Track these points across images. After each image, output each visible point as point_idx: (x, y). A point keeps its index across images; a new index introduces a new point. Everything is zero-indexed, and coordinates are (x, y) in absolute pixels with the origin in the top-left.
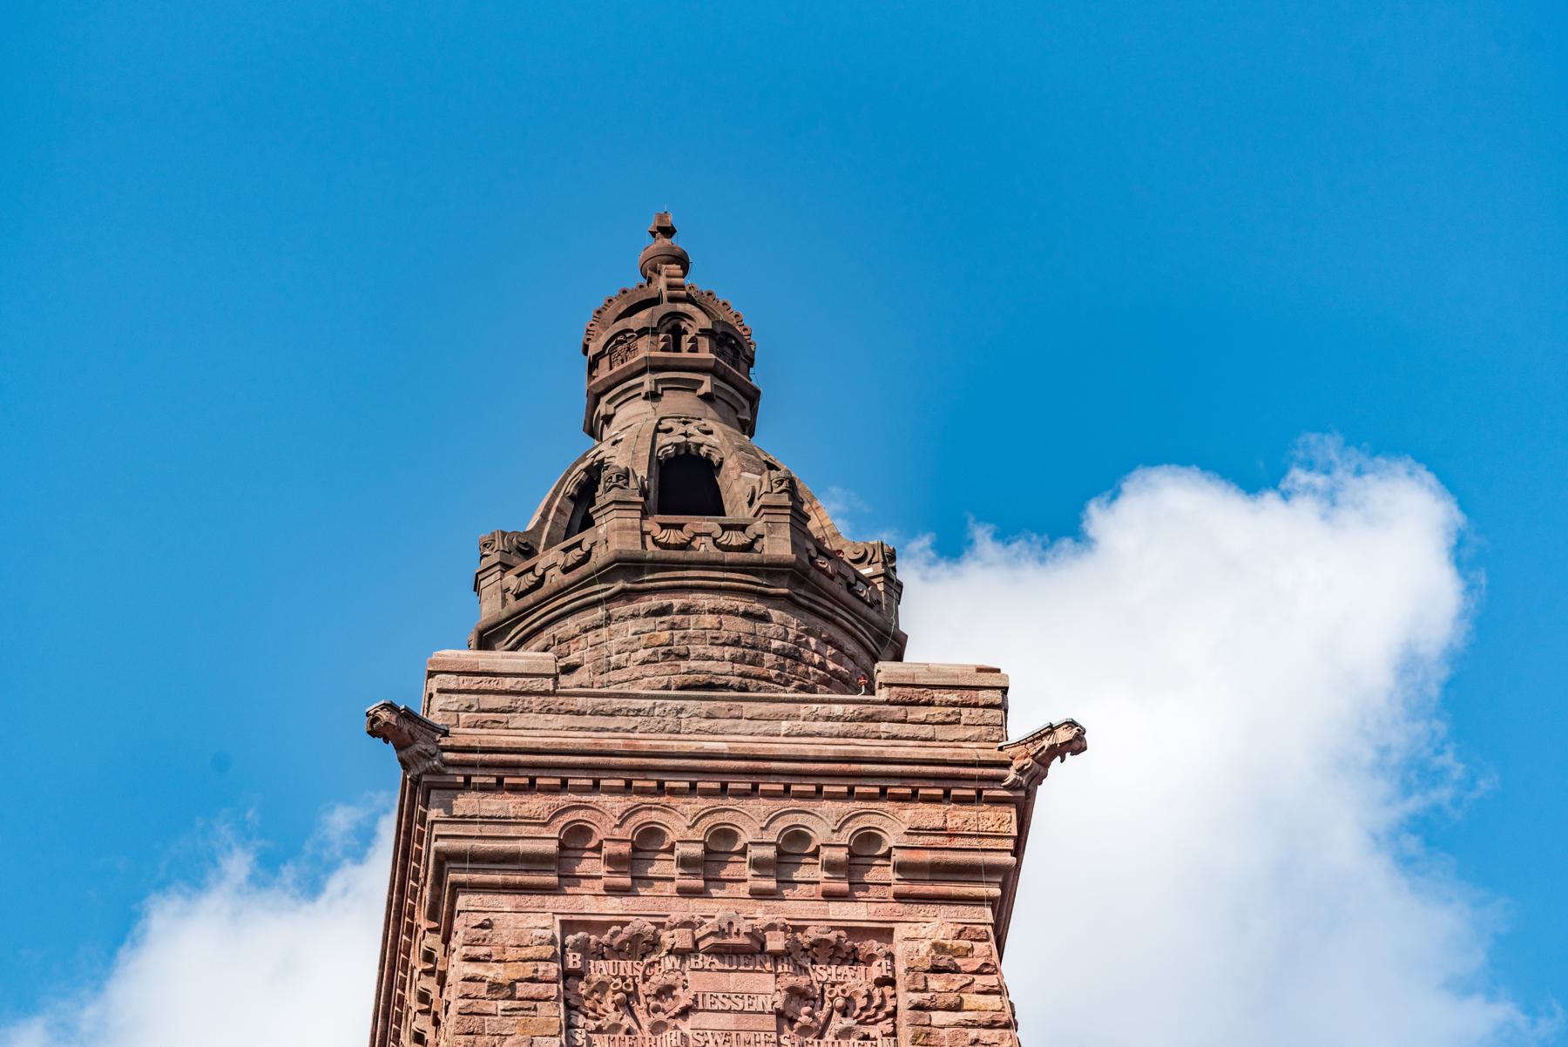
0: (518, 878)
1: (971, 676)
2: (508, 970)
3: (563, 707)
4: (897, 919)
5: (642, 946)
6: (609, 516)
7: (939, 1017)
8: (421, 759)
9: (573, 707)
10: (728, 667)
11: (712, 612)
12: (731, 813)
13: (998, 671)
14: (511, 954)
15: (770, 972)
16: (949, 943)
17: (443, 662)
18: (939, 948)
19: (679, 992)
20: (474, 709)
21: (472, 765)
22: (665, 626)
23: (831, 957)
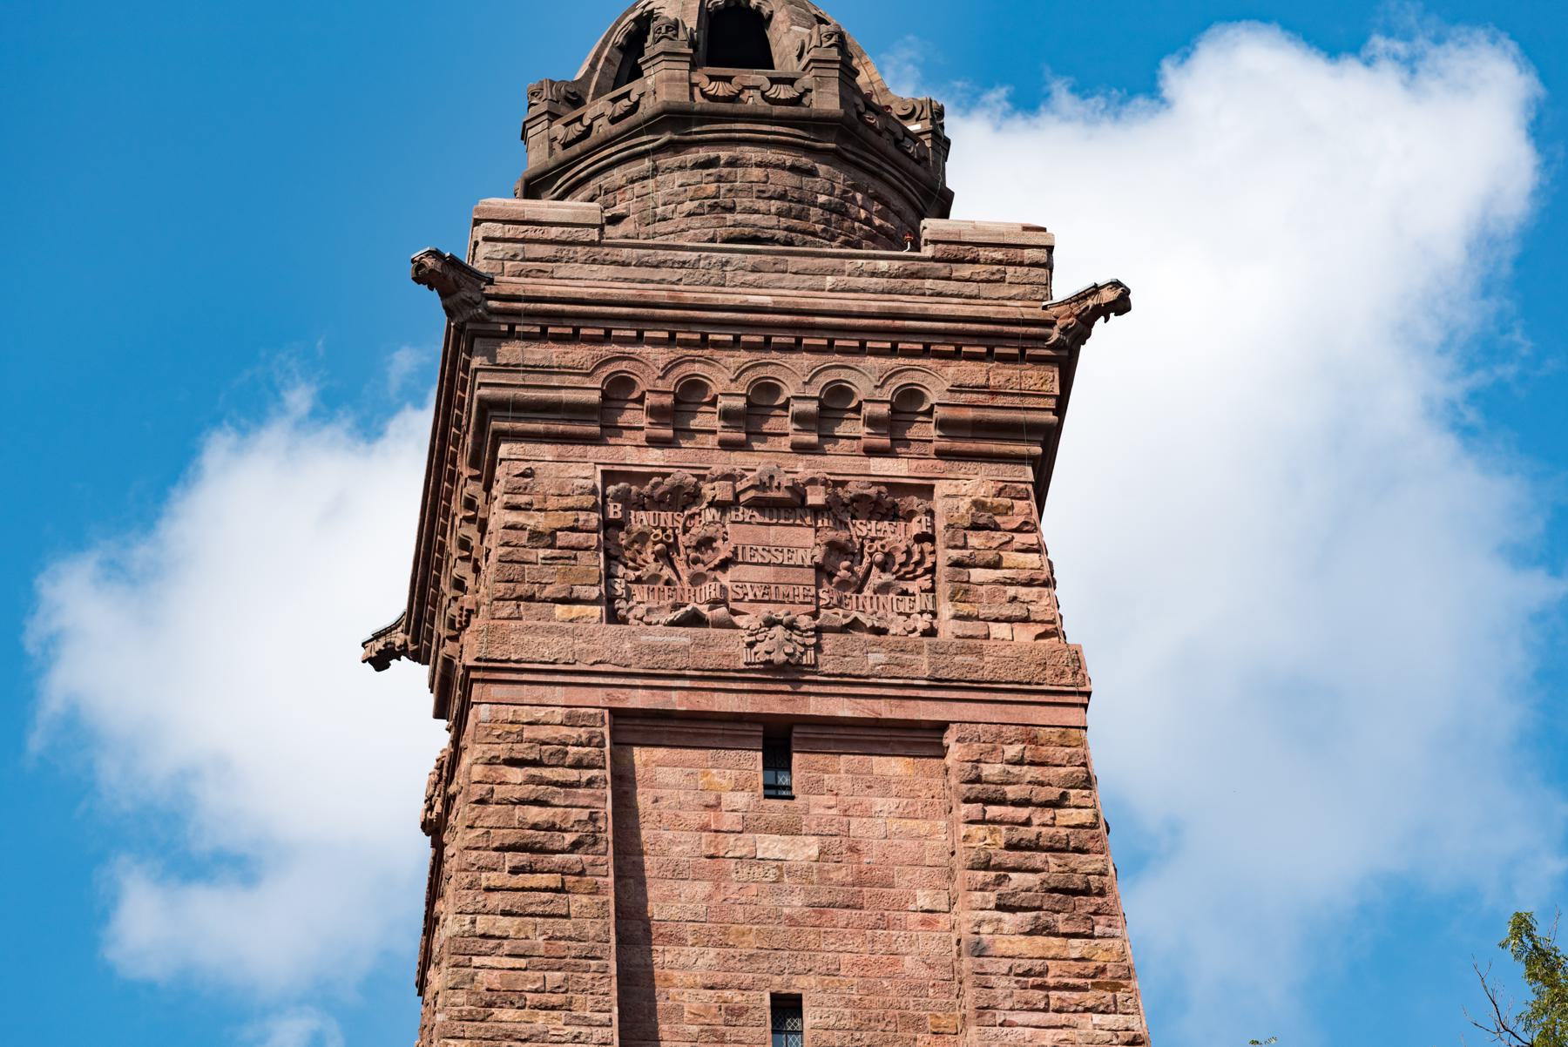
0: (561, 428)
1: (1017, 235)
2: (549, 519)
3: (608, 258)
5: (683, 498)
6: (659, 67)
7: (977, 574)
8: (465, 307)
9: (615, 258)
10: (773, 221)
11: (759, 165)
12: (774, 367)
13: (1044, 230)
14: (553, 503)
15: (810, 526)
16: (989, 500)
17: (490, 210)
18: (979, 505)
19: (718, 544)
20: (519, 258)
21: (516, 313)
22: (711, 178)
23: (870, 512)
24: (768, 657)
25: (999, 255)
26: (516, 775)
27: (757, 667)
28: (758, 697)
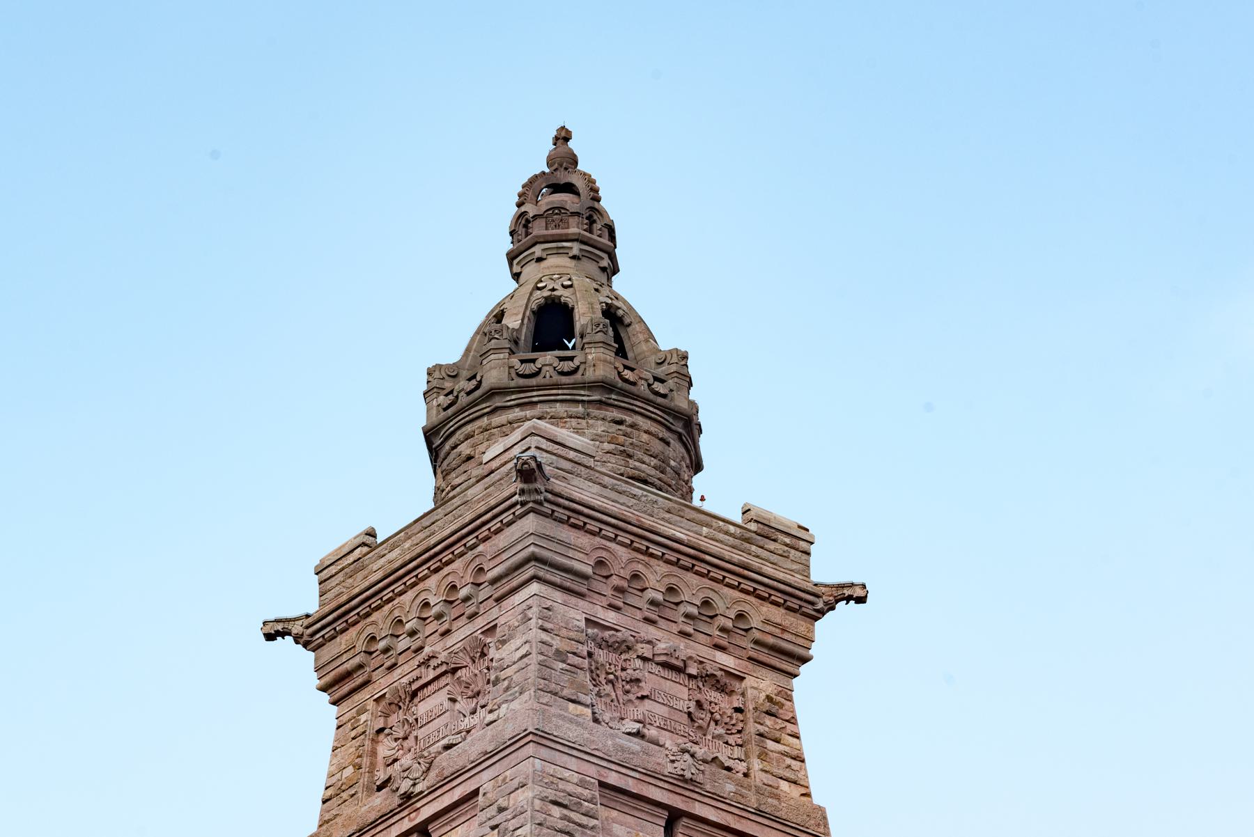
2: (563, 643)
3: (597, 479)
4: (748, 672)
5: (623, 647)
6: (598, 350)
7: (770, 745)
9: (602, 482)
11: (646, 432)
13: (807, 530)
14: (564, 632)
15: (686, 686)
17: (540, 429)
18: (769, 698)
19: (643, 684)
22: (621, 433)
23: (712, 685)
24: (682, 773)
25: (788, 540)
26: (557, 811)
27: (675, 776)
28: (671, 795)
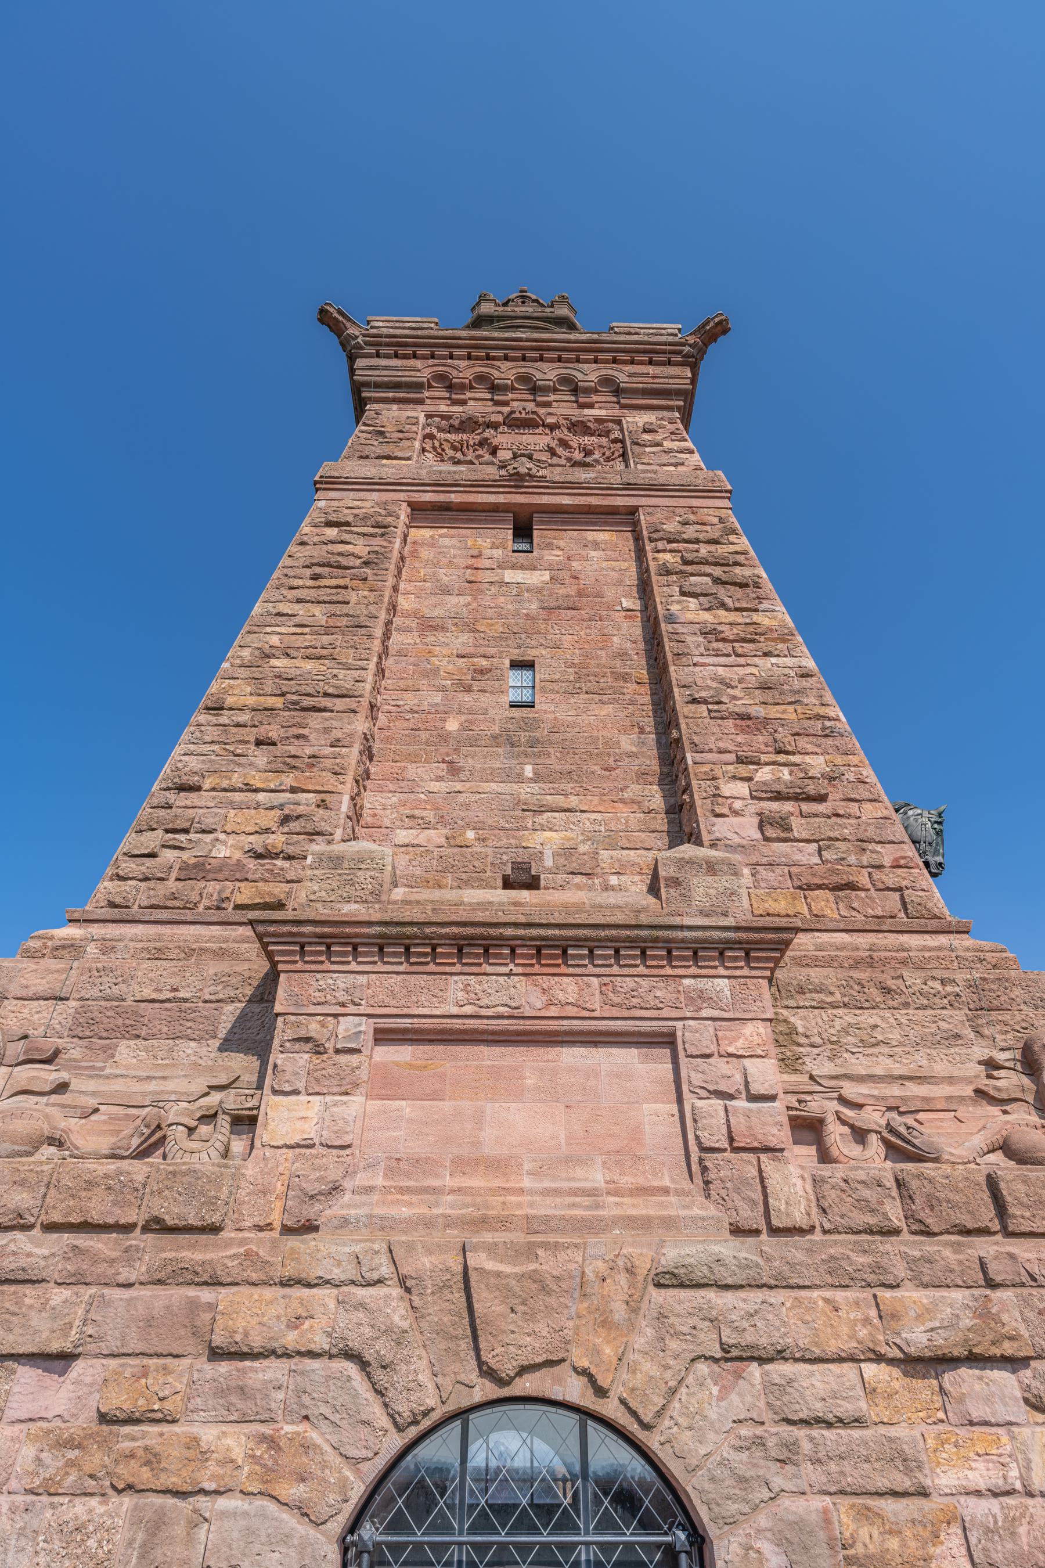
0: (402, 395)
21: (379, 344)
